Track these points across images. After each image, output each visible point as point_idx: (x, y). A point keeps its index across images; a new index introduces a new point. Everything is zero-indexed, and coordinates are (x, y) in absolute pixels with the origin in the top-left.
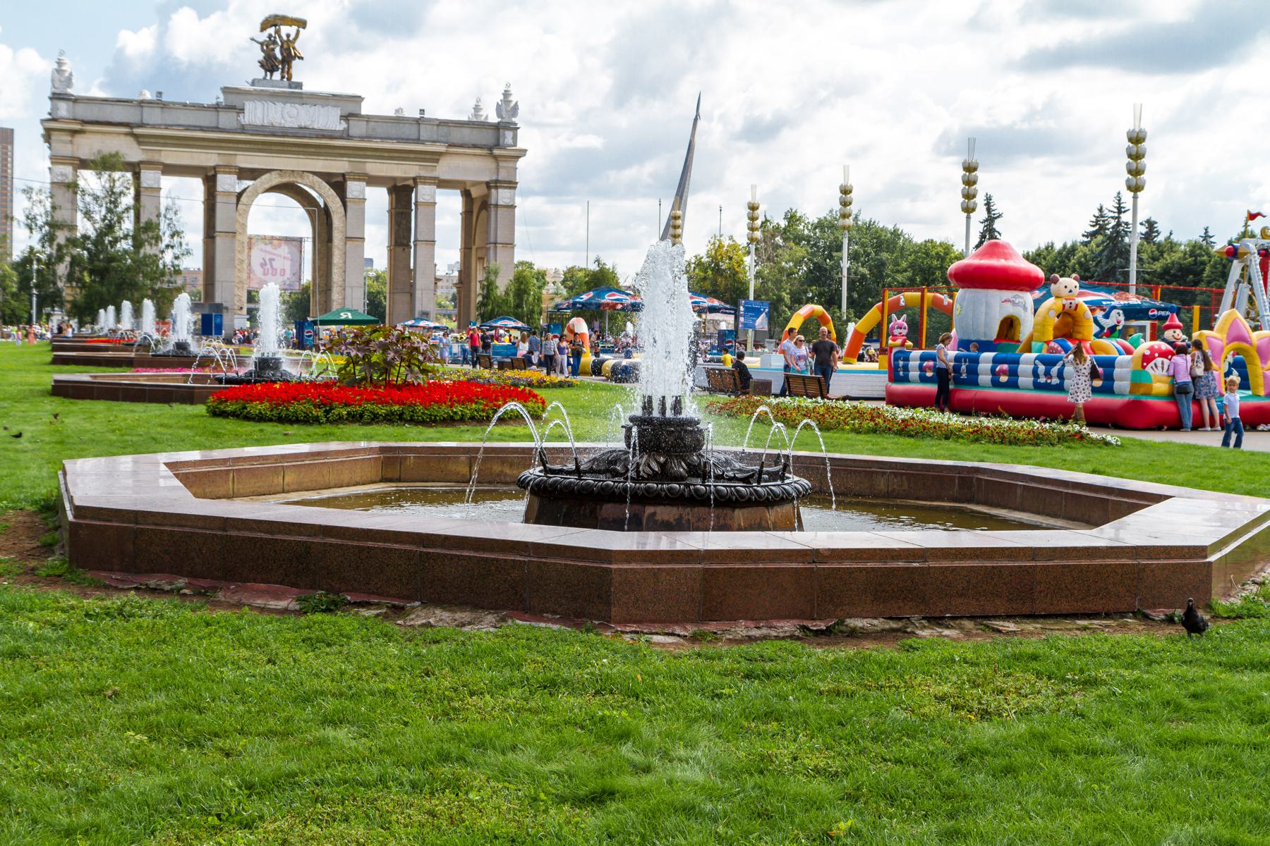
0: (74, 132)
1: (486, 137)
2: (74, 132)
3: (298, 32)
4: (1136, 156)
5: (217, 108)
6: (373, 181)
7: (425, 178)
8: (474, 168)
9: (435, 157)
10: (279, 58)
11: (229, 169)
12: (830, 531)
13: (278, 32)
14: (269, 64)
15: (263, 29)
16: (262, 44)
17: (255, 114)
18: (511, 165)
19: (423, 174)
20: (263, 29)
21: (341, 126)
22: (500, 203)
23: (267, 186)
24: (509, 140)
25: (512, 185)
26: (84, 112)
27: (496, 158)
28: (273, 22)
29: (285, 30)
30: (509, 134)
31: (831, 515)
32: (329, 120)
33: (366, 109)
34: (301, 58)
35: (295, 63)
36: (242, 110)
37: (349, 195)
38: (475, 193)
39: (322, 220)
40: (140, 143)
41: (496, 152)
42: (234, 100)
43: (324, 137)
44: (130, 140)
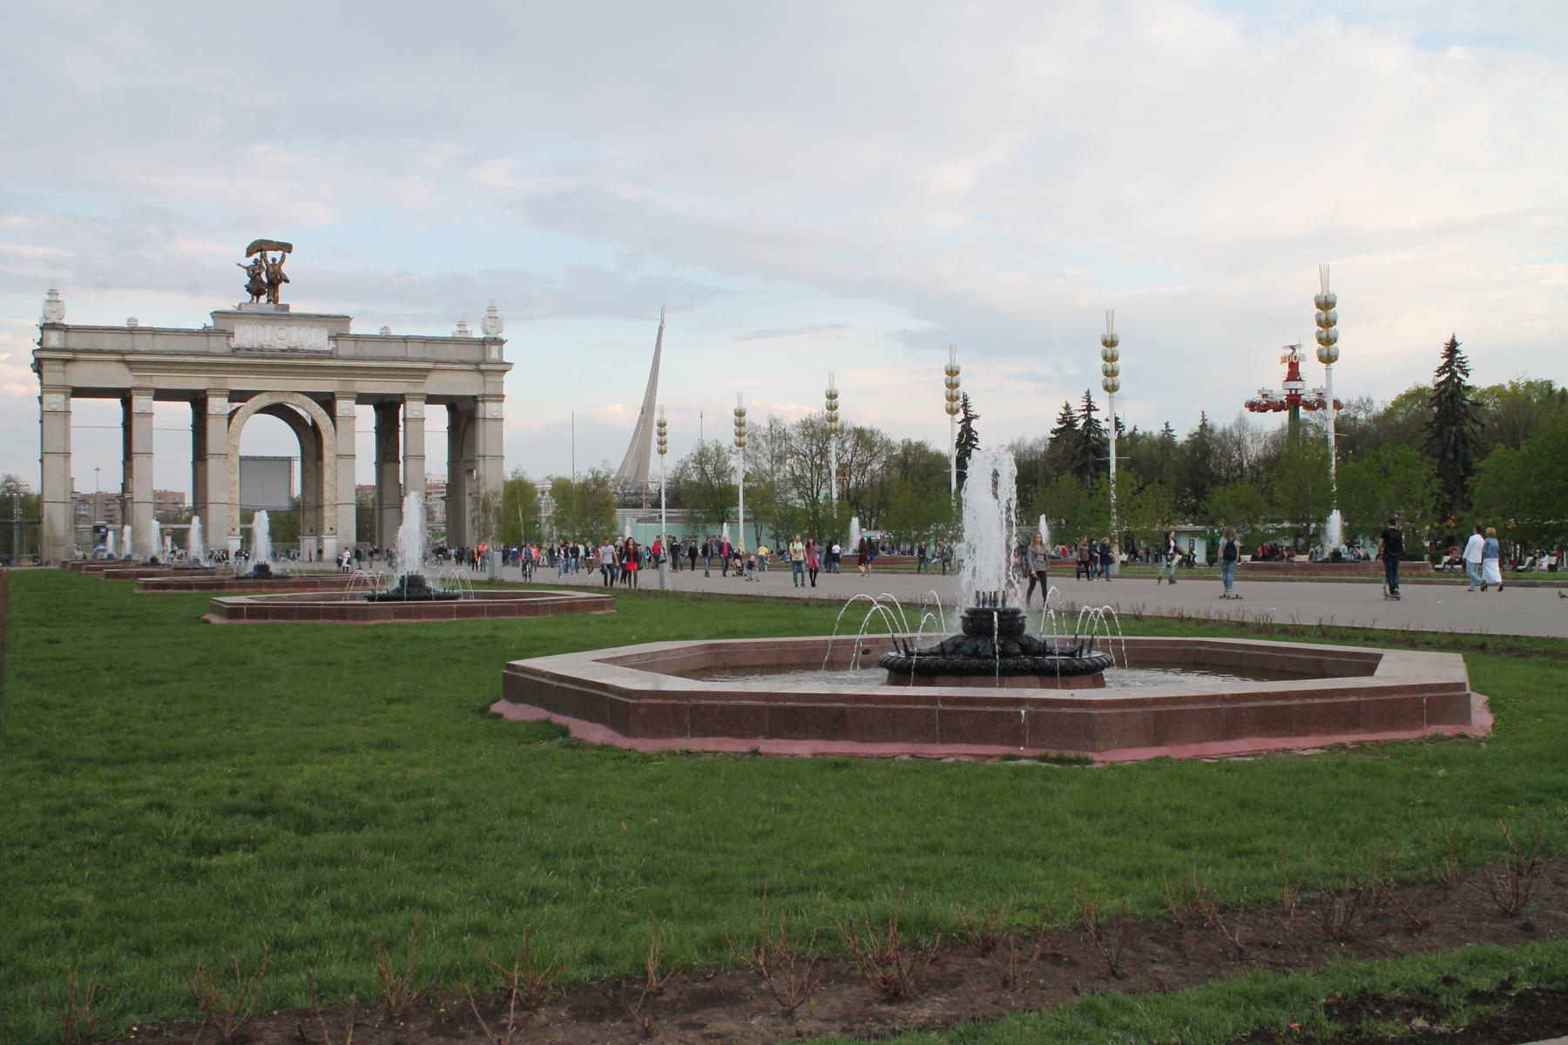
0: (67, 361)
1: (473, 353)
2: (67, 361)
3: (283, 257)
4: (1327, 323)
5: (206, 332)
8: (460, 384)
9: (423, 373)
10: (265, 281)
11: (219, 392)
12: (1130, 685)
14: (255, 289)
15: (249, 254)
17: (247, 336)
18: (497, 379)
19: (412, 390)
20: (249, 254)
21: (331, 346)
25: (500, 398)
26: (76, 341)
27: (482, 372)
28: (259, 247)
29: (270, 255)
31: (1126, 673)
32: (316, 339)
33: (355, 329)
34: (287, 281)
35: (282, 286)
37: (339, 413)
38: (462, 407)
39: (310, 436)
40: (131, 370)
41: (483, 367)
42: (225, 325)
43: (313, 358)
44: (121, 366)
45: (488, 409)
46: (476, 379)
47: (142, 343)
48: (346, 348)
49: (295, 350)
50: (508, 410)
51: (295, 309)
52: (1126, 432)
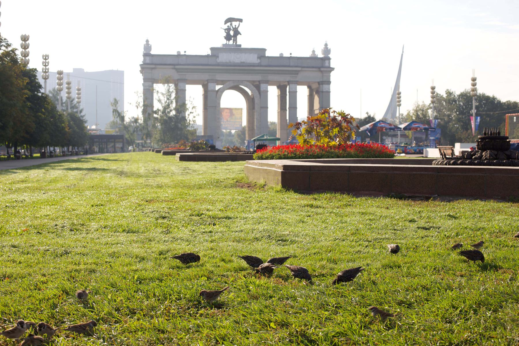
7: (292, 81)
9: (297, 73)
13: (231, 24)
14: (228, 37)
16: (225, 30)
17: (223, 58)
19: (292, 80)
22: (324, 90)
23: (228, 87)
24: (327, 64)
27: (322, 72)
28: (230, 20)
30: (327, 62)
32: (253, 59)
33: (268, 54)
35: (239, 37)
36: (218, 57)
37: (262, 89)
40: (178, 72)
43: (251, 66)
44: (174, 70)
49: (243, 63)
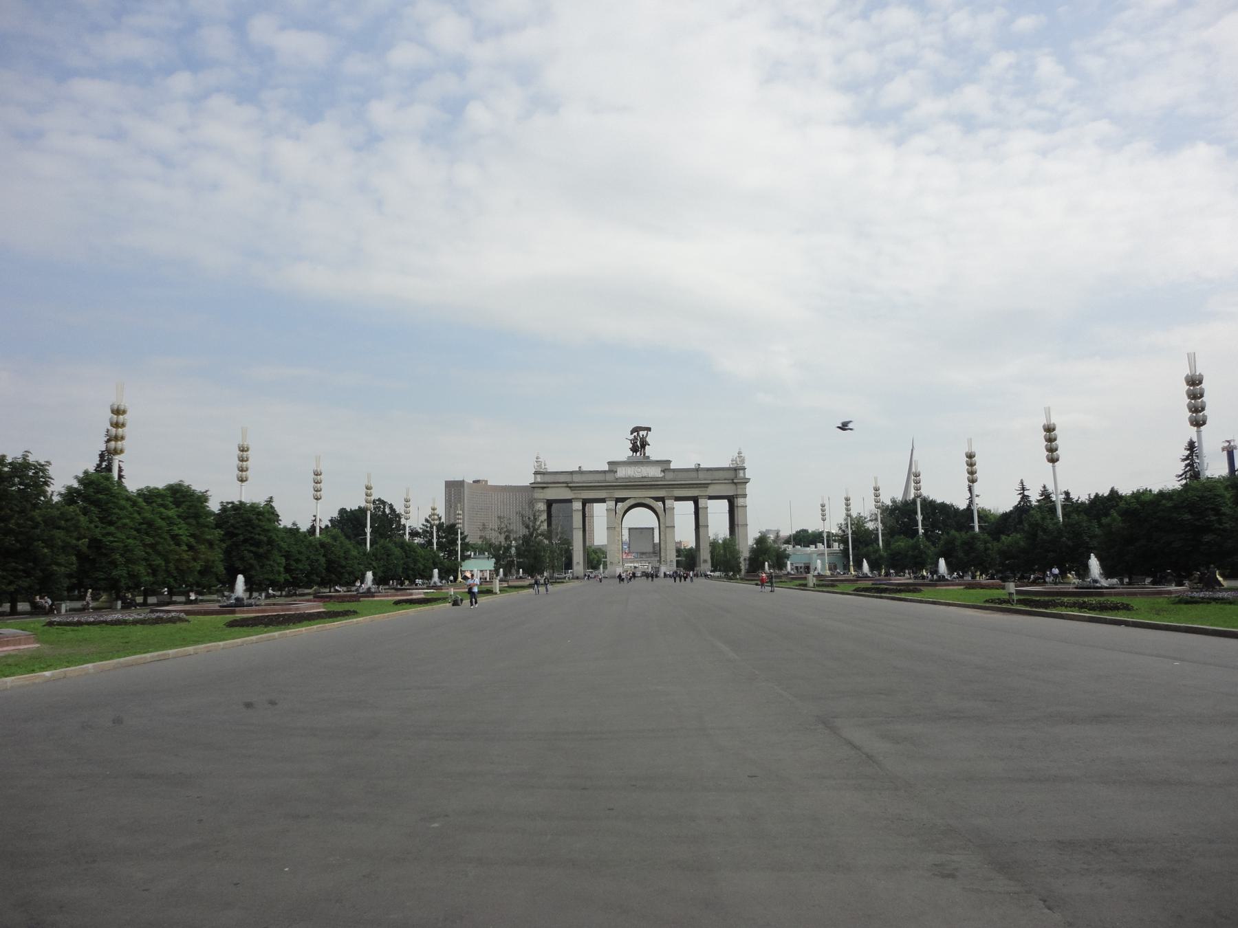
1: (731, 475)
6: (678, 499)
9: (706, 486)
10: (639, 445)
17: (622, 472)
25: (745, 496)
28: (636, 430)
29: (641, 433)
32: (655, 472)
33: (673, 466)
45: (740, 501)
46: (733, 487)
47: (576, 478)
48: (670, 476)
50: (749, 501)
51: (653, 458)
52: (854, 515)
